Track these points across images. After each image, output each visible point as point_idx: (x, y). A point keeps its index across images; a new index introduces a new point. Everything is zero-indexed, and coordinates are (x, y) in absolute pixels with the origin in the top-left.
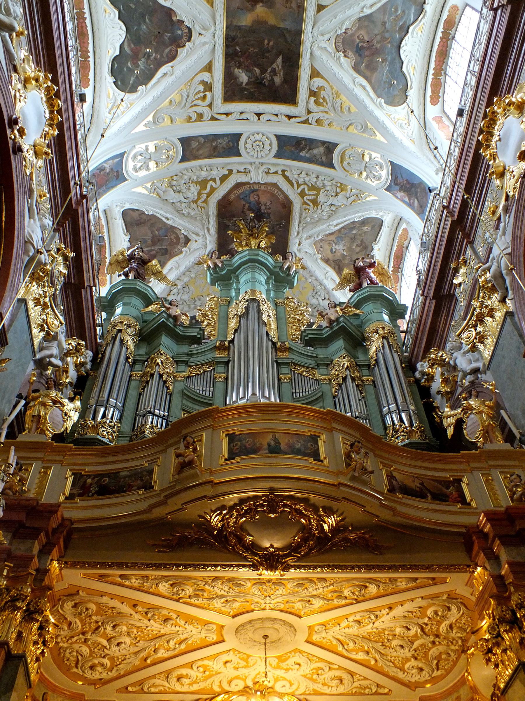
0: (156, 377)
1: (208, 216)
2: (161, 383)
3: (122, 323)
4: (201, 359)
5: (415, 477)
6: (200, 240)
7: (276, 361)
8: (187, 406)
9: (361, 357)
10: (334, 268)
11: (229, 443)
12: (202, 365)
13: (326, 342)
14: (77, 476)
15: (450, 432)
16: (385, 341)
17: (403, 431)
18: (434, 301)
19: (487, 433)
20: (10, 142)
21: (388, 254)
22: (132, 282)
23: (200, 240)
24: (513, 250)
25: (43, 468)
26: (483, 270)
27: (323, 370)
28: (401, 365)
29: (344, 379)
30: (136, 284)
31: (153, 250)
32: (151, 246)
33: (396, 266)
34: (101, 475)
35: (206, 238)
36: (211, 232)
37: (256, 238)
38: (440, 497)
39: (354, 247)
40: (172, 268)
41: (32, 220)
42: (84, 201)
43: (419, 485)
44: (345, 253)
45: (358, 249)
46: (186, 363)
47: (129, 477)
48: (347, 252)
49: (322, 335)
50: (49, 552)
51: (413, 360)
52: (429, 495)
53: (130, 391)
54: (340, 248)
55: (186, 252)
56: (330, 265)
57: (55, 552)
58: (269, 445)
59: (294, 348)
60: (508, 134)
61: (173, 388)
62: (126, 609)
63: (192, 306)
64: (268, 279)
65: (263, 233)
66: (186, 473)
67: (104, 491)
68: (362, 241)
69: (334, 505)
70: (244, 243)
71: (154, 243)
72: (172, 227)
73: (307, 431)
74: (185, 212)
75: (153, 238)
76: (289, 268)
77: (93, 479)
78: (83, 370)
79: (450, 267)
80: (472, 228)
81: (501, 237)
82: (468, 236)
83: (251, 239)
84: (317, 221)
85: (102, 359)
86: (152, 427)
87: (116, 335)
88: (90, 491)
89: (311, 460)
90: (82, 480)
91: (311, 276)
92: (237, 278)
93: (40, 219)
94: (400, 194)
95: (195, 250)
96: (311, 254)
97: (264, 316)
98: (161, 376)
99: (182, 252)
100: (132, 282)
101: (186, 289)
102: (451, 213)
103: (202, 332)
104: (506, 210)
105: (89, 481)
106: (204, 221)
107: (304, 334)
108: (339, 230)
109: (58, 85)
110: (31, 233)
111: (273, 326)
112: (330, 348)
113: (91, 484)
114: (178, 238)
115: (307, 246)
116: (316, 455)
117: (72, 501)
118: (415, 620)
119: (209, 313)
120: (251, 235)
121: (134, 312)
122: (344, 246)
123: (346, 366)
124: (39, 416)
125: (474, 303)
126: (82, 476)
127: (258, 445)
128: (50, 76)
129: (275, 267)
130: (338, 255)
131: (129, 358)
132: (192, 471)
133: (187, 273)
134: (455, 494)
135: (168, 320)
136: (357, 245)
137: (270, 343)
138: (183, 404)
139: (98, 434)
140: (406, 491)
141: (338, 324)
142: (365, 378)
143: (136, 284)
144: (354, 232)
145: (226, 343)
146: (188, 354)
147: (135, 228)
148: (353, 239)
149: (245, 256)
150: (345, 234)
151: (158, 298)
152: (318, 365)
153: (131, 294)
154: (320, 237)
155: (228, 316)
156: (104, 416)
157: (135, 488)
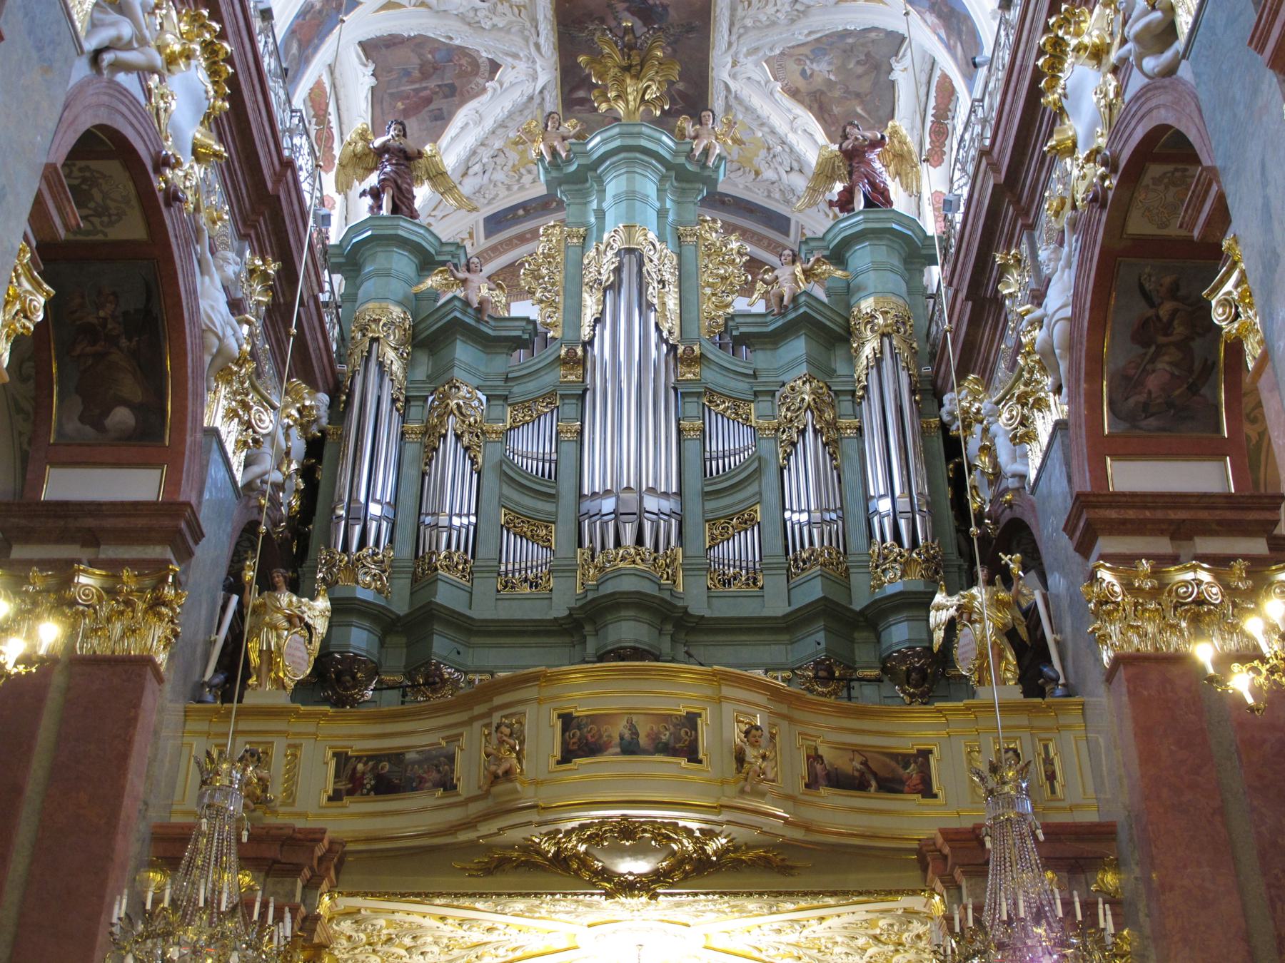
0: (451, 438)
1: (535, 22)
2: (460, 451)
3: (377, 321)
4: (531, 386)
5: (857, 750)
6: (522, 66)
7: (676, 389)
8: (508, 498)
10: (810, 109)
11: (564, 731)
12: (535, 400)
14: (342, 759)
15: (939, 636)
16: (886, 341)
17: (895, 560)
18: (970, 303)
20: (160, 196)
21: (924, 79)
22: (389, 223)
23: (522, 66)
24: (1073, 313)
25: (289, 746)
26: (1031, 323)
27: (764, 405)
28: (913, 392)
29: (802, 432)
30: (397, 227)
31: (425, 88)
32: (421, 80)
33: (942, 106)
34: (376, 758)
35: (534, 62)
36: (543, 50)
37: (637, 77)
38: (890, 785)
39: (851, 66)
40: (467, 124)
41: (207, 278)
42: (289, 173)
43: (859, 766)
44: (833, 78)
45: (860, 70)
46: (505, 398)
47: (420, 763)
48: (836, 75)
49: (766, 324)
50: (317, 887)
51: (940, 382)
52: (874, 783)
53: (405, 470)
54: (822, 69)
55: (495, 90)
56: (801, 102)
57: (325, 886)
58: (622, 738)
59: (710, 356)
60: (1079, 87)
61: (484, 457)
62: (428, 922)
63: (516, 188)
64: (663, 179)
65: (653, 65)
67: (385, 787)
68: (868, 55)
69: (717, 829)
70: (612, 94)
71: (425, 76)
72: (459, 47)
74: (488, 25)
75: (422, 66)
76: (706, 152)
77: (366, 764)
78: (314, 431)
79: (994, 262)
80: (1033, 201)
81: (1063, 271)
82: (1027, 214)
83: (628, 81)
84: (768, 26)
85: (349, 403)
86: (449, 557)
87: (369, 352)
88: (363, 786)
89: (683, 762)
90: (350, 767)
91: (762, 124)
92: (600, 180)
93: (220, 268)
94: (931, 18)
95: (512, 85)
96: (759, 82)
97: (651, 289)
98: (458, 437)
99: (484, 90)
100: (389, 223)
101: (500, 160)
102: (994, 166)
103: (531, 327)
104: (1073, 225)
105: (360, 767)
106: (526, 33)
107: (731, 323)
108: (817, 40)
109: (220, 20)
110: (210, 311)
111: (672, 303)
113: (364, 773)
114: (475, 63)
115: (750, 66)
116: (691, 753)
117: (339, 803)
118: (862, 931)
119: (544, 271)
120: (627, 69)
121: (398, 288)
122: (830, 64)
123: (805, 405)
126: (348, 758)
127: (605, 739)
128: (205, 13)
129: (676, 153)
130: (818, 82)
131: (398, 400)
132: (509, 786)
133: (499, 131)
135: (464, 313)
136: (858, 62)
137: (664, 347)
138: (501, 496)
139: (357, 582)
140: (838, 781)
141: (796, 308)
142: (843, 422)
143: (397, 227)
144: (850, 41)
145: (579, 351)
146: (507, 379)
147: (384, 51)
148: (848, 52)
149: (612, 138)
150: (832, 44)
151: (442, 244)
152: (756, 394)
153: (388, 245)
154: (777, 52)
155: (582, 276)
156: (363, 543)
157: (429, 784)
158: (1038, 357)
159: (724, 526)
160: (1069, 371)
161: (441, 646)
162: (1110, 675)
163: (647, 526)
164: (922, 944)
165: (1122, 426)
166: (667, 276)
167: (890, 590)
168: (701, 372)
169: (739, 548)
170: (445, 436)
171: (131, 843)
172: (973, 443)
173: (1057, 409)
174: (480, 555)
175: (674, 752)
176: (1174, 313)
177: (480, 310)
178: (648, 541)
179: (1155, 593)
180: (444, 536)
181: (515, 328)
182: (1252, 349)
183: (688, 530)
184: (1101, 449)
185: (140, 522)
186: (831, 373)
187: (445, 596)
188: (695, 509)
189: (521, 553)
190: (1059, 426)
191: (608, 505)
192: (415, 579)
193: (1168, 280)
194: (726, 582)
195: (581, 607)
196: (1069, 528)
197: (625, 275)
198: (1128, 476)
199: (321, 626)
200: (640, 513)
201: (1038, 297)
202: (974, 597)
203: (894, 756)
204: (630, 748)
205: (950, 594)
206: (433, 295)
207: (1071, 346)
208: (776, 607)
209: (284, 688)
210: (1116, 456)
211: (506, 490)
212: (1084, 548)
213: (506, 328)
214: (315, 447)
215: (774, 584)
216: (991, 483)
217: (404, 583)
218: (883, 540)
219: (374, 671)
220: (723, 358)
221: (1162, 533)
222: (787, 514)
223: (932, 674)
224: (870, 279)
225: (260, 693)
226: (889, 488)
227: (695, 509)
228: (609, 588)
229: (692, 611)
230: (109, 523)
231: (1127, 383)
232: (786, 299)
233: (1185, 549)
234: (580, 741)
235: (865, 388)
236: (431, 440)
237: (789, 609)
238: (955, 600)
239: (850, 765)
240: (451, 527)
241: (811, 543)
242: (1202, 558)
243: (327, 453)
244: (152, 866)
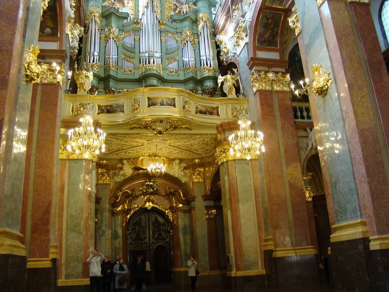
0: (111, 39)
2: (114, 42)
5: (205, 106)
9: (195, 28)
13: (182, 21)
15: (220, 85)
18: (225, 17)
19: (230, 89)
27: (179, 35)
28: (210, 34)
29: (187, 42)
38: (211, 113)
66: (136, 111)
67: (109, 112)
73: (172, 97)
105: (103, 108)
111: (159, 11)
112: (182, 24)
116: (174, 106)
124: (82, 83)
125: (237, 29)
134: (216, 112)
138: (123, 52)
140: (201, 112)
145: (139, 21)
158: (242, 29)
159: (171, 60)
160: (250, 32)
161: (112, 83)
162: (255, 94)
163: (155, 60)
164: (212, 145)
165: (259, 44)
166: (158, 6)
167: (206, 75)
168: (164, 27)
169: (173, 66)
170: (110, 38)
171: (58, 123)
172: (222, 46)
173: (247, 40)
174: (119, 64)
175: (171, 106)
176: (272, 22)
177: (117, 10)
178: (155, 63)
179: (265, 78)
180: (111, 60)
181: (125, 15)
182: (297, 32)
183: (163, 60)
184: (255, 49)
185: (55, 54)
186: (193, 29)
187: (112, 73)
188: (164, 57)
189: (128, 65)
190: (247, 44)
191: (147, 55)
192: (105, 69)
193: (271, 15)
194: (171, 72)
195: (142, 76)
196: (248, 64)
197: (149, 4)
198: (261, 55)
199: (91, 78)
200: (153, 57)
201: (243, 16)
202: (227, 77)
203: (212, 108)
204: (162, 104)
205: (222, 76)
206: (105, 6)
207: (250, 27)
208: (182, 78)
209: (85, 90)
210: (258, 50)
211: (124, 51)
212: (251, 69)
213: (123, 15)
214: (81, 40)
215: (181, 73)
216: (226, 55)
217: (103, 70)
218: (204, 65)
219: (97, 89)
220: (169, 24)
221: (266, 66)
222: (184, 59)
223: (217, 91)
224: (202, 9)
225: (80, 92)
226: (207, 53)
227: (164, 57)
228: (148, 72)
229: (165, 78)
230: (47, 54)
231: (261, 36)
232: (185, 13)
233: (270, 70)
234: (152, 103)
235: (200, 33)
236: (107, 39)
237: (184, 79)
238: (224, 77)
239: (204, 109)
240: (112, 58)
241: (189, 65)
242: (274, 72)
243: (84, 41)
244: (62, 127)
